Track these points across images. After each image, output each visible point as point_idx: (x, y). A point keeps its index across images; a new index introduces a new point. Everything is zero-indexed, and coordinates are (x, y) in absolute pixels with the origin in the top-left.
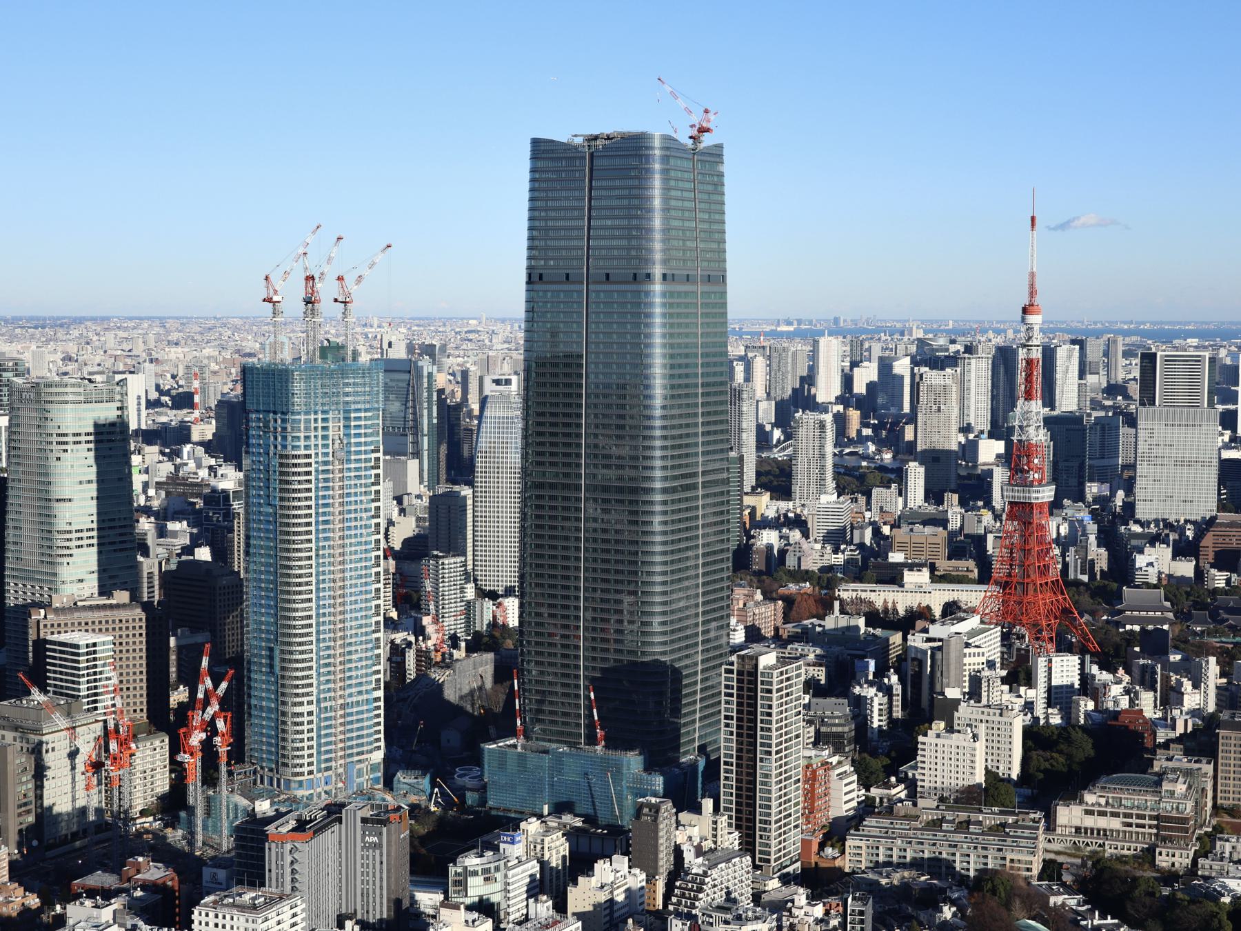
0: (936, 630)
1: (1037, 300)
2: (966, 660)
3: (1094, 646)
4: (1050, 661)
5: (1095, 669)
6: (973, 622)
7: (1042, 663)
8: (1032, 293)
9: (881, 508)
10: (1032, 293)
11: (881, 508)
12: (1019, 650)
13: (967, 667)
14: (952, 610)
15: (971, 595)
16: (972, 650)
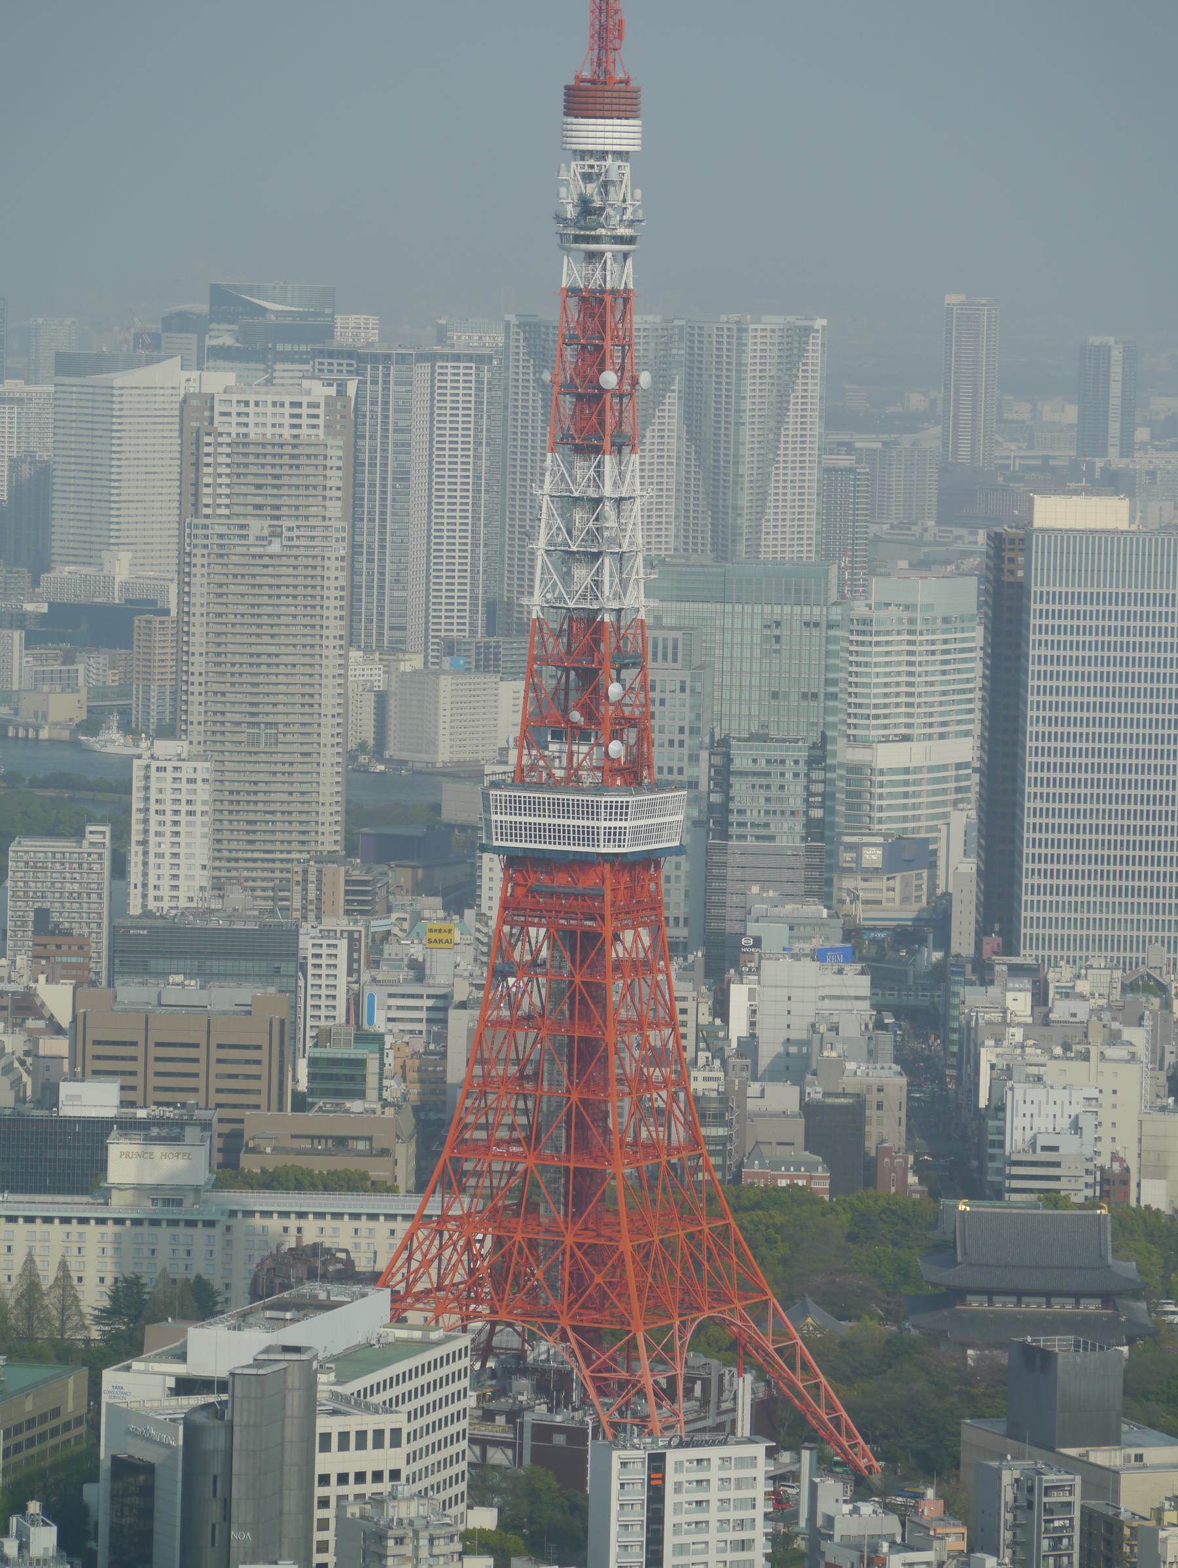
0: (220, 1348)
1: (629, 62)
2: (327, 1462)
3: (826, 1402)
4: (657, 1463)
5: (832, 1496)
6: (363, 1317)
7: (621, 1474)
8: (606, 33)
9: (42, 916)
10: (606, 33)
11: (42, 916)
12: (543, 1432)
13: (332, 1491)
14: (294, 1279)
15: (366, 1233)
16: (353, 1423)
